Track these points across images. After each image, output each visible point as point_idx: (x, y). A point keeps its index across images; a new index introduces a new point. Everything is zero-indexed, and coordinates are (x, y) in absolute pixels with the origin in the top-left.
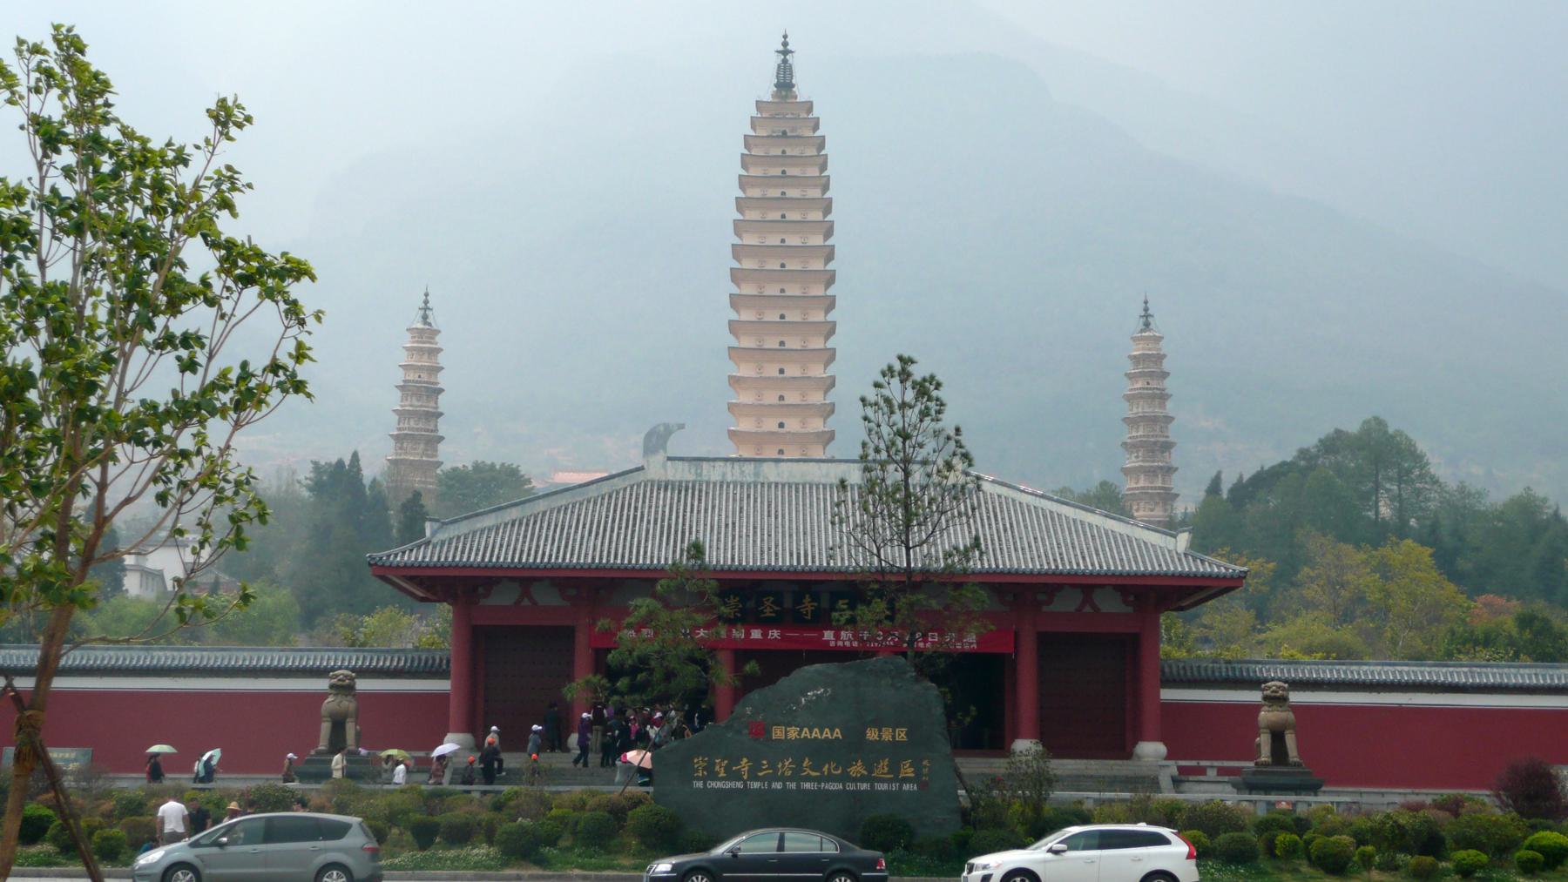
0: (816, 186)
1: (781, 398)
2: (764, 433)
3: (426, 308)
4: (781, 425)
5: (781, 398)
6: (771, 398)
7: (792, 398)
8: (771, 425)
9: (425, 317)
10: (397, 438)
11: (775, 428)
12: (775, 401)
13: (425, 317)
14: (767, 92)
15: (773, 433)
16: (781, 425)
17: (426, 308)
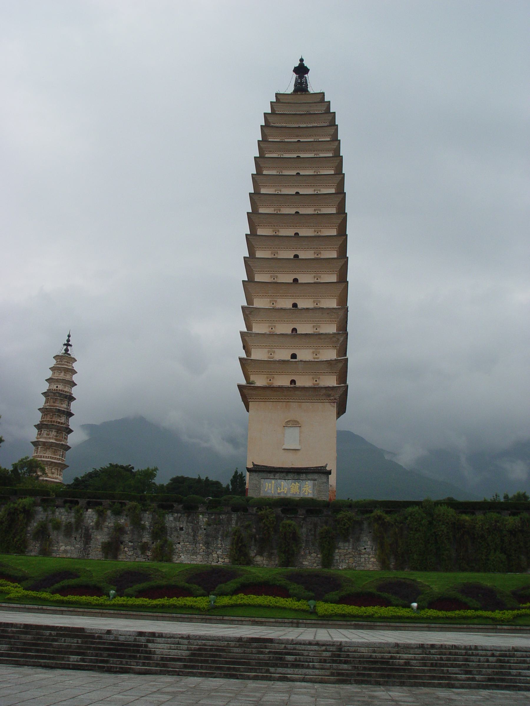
0: (328, 151)
1: (294, 330)
2: (275, 361)
3: (68, 345)
4: (294, 356)
5: (294, 330)
6: (285, 328)
7: (304, 329)
8: (284, 355)
9: (67, 350)
10: (39, 427)
11: (288, 358)
12: (290, 332)
13: (67, 350)
14: (288, 86)
15: (284, 362)
16: (294, 356)
17: (68, 345)
